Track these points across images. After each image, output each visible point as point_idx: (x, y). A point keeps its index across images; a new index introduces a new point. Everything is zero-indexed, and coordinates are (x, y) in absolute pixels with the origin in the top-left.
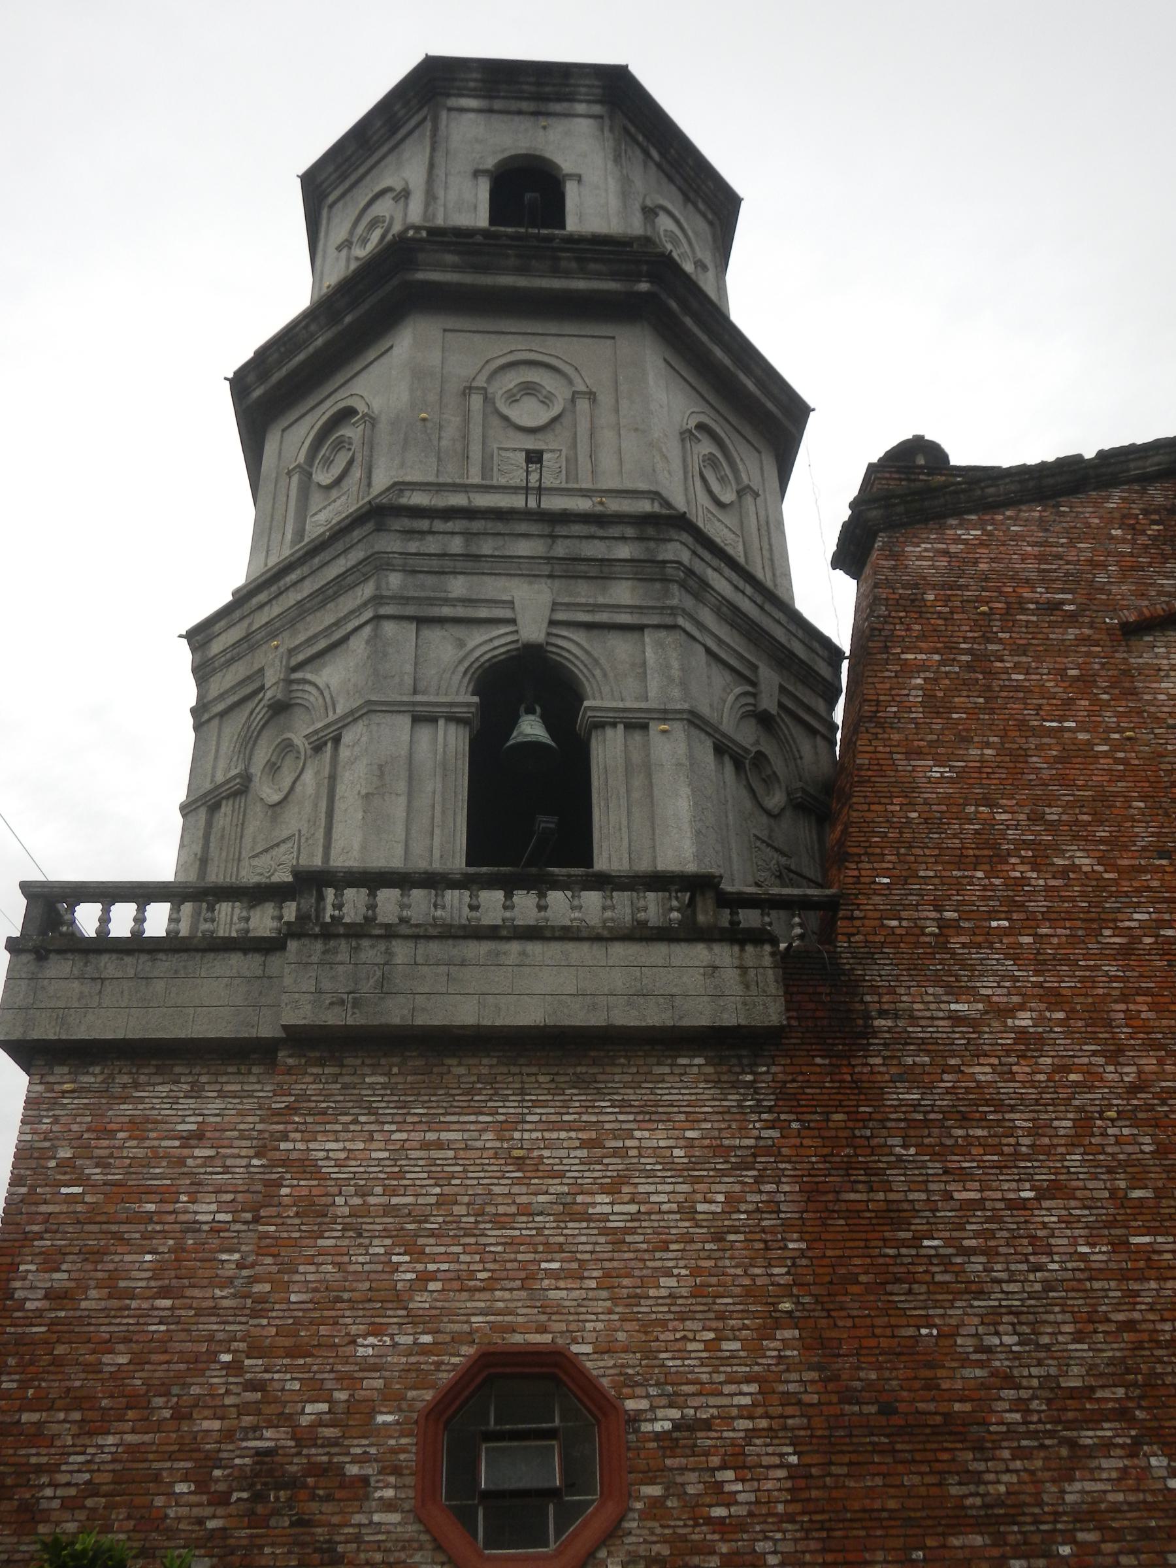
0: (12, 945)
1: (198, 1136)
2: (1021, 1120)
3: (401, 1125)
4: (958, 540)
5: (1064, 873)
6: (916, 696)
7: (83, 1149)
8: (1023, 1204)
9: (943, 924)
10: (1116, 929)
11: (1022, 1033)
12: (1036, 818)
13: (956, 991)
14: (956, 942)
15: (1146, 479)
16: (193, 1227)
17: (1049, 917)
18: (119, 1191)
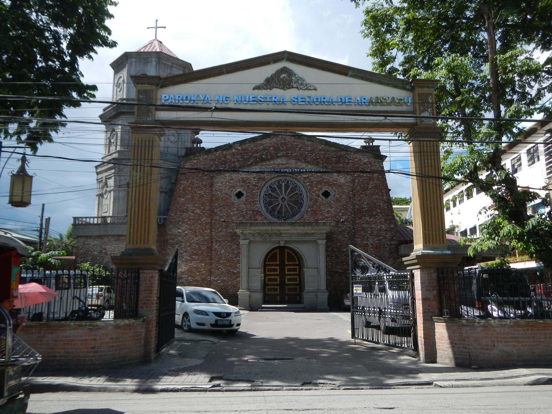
0: (72, 224)
1: (94, 245)
2: (183, 244)
3: (115, 245)
4: (193, 162)
5: (195, 214)
6: (182, 188)
7: (83, 247)
8: (181, 253)
9: (179, 221)
10: (201, 221)
11: (186, 234)
12: (194, 206)
13: (179, 229)
14: (180, 223)
15: (223, 150)
16: (94, 255)
17: (193, 219)
18: (87, 251)
